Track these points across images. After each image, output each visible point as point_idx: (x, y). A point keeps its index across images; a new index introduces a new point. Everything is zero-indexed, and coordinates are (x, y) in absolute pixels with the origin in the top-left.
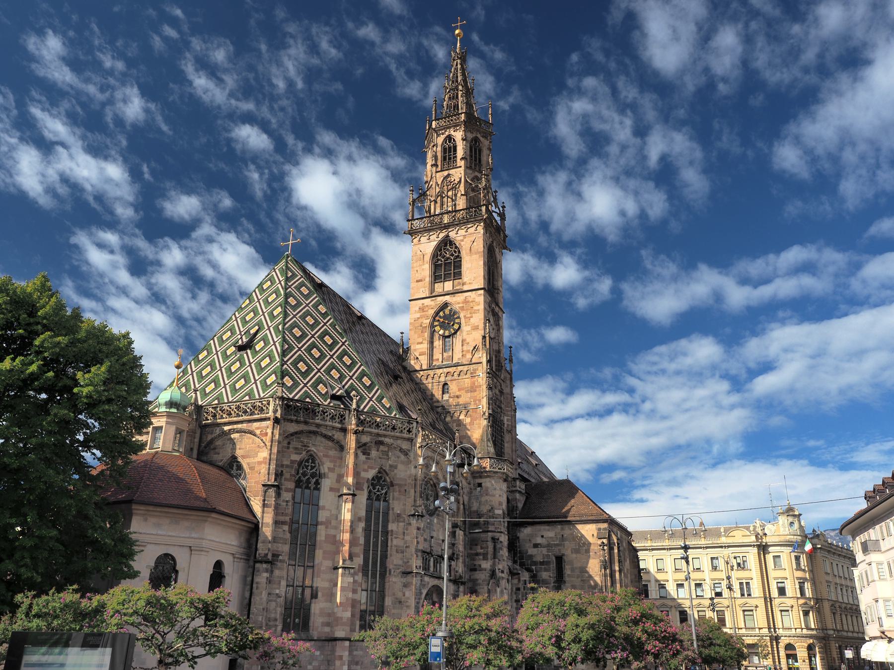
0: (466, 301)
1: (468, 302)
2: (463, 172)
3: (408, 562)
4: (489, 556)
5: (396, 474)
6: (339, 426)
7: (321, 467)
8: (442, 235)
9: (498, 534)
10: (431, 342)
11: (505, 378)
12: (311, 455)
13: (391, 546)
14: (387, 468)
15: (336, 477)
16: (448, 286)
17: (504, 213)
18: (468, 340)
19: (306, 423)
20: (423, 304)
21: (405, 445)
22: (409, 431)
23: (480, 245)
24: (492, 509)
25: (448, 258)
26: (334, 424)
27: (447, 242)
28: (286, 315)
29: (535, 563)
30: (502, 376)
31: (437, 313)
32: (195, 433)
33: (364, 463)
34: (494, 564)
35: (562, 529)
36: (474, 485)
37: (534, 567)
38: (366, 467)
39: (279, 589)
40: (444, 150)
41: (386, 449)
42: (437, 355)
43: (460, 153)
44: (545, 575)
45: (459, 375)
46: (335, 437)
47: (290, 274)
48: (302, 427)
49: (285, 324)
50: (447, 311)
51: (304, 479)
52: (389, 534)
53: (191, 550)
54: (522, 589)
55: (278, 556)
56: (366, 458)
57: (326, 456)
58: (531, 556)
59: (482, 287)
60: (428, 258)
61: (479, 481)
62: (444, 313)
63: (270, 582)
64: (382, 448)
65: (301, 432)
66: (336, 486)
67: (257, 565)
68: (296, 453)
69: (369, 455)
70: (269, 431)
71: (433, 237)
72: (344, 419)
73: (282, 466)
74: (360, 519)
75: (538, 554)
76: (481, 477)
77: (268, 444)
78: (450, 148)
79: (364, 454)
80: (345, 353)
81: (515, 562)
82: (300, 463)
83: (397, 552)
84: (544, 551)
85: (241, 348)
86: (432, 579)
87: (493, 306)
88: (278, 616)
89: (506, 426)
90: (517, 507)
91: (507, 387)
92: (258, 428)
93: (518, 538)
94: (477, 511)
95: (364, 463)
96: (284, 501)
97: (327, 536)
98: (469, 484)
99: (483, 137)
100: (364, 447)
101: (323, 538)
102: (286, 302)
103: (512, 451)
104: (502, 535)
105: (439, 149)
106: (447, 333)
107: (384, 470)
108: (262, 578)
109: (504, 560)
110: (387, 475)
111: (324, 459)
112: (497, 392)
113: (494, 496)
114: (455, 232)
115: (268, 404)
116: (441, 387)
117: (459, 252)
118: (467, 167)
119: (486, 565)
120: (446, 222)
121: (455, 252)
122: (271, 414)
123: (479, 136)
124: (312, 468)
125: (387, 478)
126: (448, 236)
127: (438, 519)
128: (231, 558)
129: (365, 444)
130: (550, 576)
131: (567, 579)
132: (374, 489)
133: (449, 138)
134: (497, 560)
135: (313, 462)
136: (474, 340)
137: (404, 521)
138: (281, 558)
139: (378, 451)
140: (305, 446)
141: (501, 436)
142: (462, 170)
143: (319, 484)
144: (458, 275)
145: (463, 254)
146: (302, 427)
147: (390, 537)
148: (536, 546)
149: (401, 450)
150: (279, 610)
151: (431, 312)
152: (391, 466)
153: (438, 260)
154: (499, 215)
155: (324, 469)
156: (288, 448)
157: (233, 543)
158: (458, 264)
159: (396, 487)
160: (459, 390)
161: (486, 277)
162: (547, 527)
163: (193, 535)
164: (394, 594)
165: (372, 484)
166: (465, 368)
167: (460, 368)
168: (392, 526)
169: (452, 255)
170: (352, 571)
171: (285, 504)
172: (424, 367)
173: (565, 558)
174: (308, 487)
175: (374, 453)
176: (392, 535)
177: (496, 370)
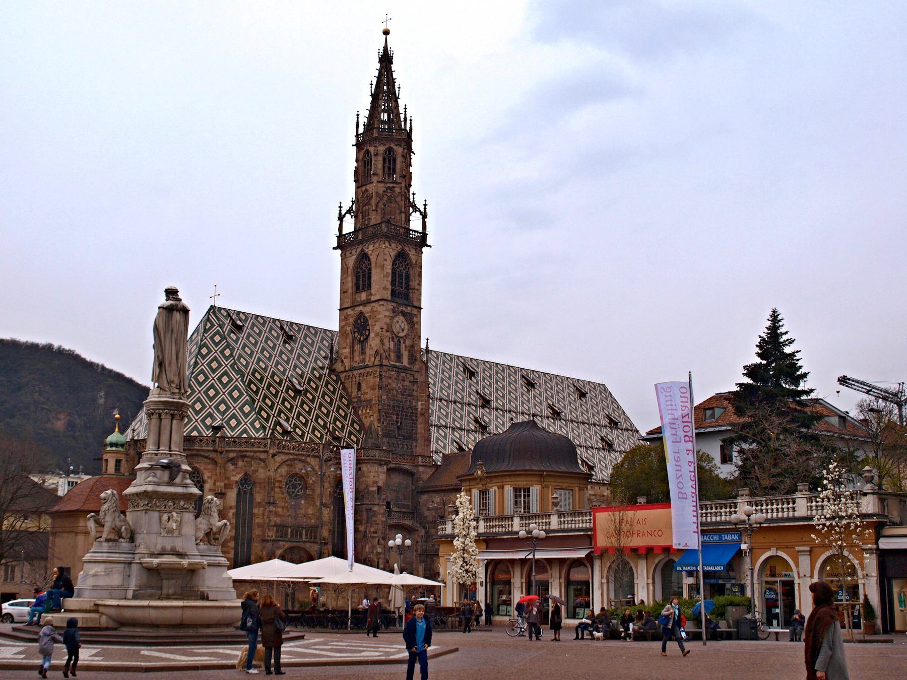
0: (372, 311)
4: (364, 522)
5: (257, 476)
9: (371, 506)
10: (353, 347)
11: (421, 368)
12: (196, 469)
15: (213, 482)
16: (363, 296)
18: (373, 345)
21: (263, 456)
22: (265, 445)
24: (367, 486)
26: (208, 448)
28: (196, 364)
29: (428, 522)
31: (356, 321)
33: (233, 470)
42: (357, 358)
45: (367, 376)
46: (211, 456)
47: (209, 325)
49: (192, 373)
64: (246, 459)
66: (213, 487)
71: (354, 252)
74: (231, 508)
80: (236, 388)
81: (417, 521)
83: (258, 527)
86: (289, 543)
89: (419, 410)
95: (233, 470)
99: (396, 145)
102: (199, 353)
106: (362, 339)
113: (368, 477)
114: (366, 247)
120: (360, 238)
123: (392, 145)
124: (198, 477)
126: (362, 250)
129: (232, 459)
132: (242, 487)
133: (368, 152)
134: (369, 525)
135: (198, 473)
136: (376, 345)
141: (413, 420)
145: (373, 265)
149: (260, 459)
151: (351, 320)
152: (253, 471)
153: (358, 272)
154: (421, 213)
155: (205, 477)
158: (370, 278)
160: (367, 388)
164: (256, 553)
165: (241, 484)
167: (367, 370)
168: (255, 511)
172: (347, 369)
175: (240, 463)
177: (409, 363)
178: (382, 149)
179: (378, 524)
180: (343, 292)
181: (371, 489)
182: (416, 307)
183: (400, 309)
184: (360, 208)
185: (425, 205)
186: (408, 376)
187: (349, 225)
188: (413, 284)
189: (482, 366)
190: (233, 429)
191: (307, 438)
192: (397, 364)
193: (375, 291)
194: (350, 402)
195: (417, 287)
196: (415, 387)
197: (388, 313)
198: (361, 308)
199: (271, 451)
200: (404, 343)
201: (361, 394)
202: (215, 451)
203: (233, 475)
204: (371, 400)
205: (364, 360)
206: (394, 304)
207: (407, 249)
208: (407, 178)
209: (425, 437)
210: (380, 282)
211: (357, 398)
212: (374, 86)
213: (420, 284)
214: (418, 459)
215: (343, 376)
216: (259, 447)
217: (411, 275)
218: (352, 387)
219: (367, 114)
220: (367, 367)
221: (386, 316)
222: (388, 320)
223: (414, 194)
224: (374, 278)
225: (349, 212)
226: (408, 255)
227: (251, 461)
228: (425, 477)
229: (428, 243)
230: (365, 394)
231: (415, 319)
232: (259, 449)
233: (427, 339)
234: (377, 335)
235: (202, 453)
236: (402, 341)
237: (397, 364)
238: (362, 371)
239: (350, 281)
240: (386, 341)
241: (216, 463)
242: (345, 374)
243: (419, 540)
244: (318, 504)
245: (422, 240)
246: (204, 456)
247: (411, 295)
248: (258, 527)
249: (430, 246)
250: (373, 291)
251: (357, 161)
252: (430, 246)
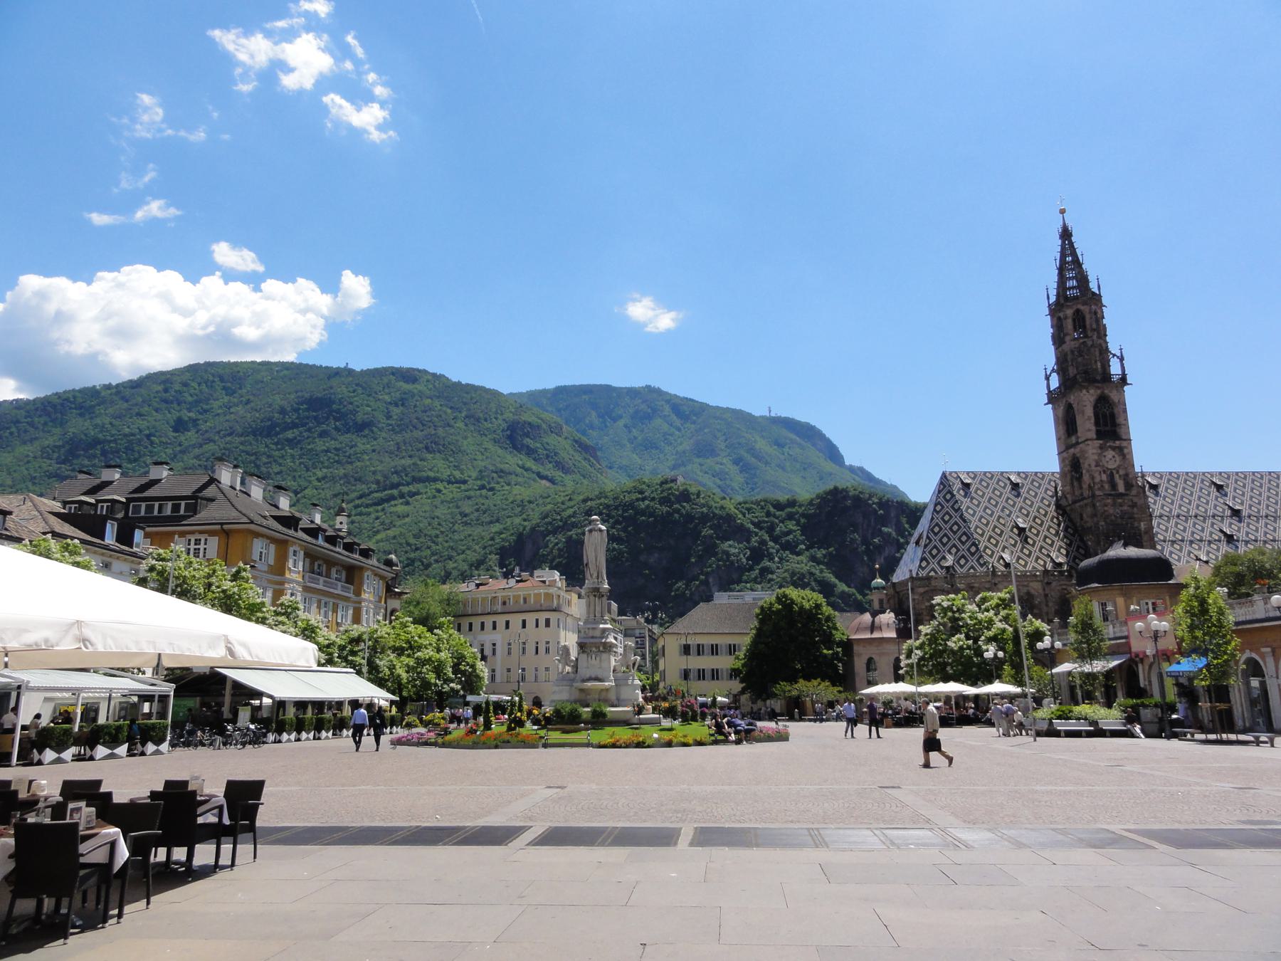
8: (1064, 402)
11: (1138, 493)
16: (1073, 439)
28: (932, 519)
42: (1077, 493)
48: (927, 588)
60: (1060, 421)
102: (935, 510)
144: (1076, 431)
145: (1076, 412)
151: (1067, 462)
154: (1118, 357)
167: (1085, 501)
177: (1126, 490)
178: (1069, 312)
180: (1058, 439)
182: (1125, 440)
184: (1062, 365)
185: (1121, 349)
187: (1055, 382)
188: (1120, 420)
189: (1233, 478)
190: (962, 567)
191: (1029, 567)
192: (1113, 492)
194: (1076, 530)
195: (1124, 422)
196: (1135, 509)
197: (1095, 451)
198: (1072, 451)
200: (1118, 472)
204: (1091, 527)
205: (1082, 494)
206: (1101, 442)
207: (1106, 391)
208: (1101, 332)
210: (1087, 425)
212: (1058, 261)
213: (1126, 419)
215: (1068, 508)
219: (1055, 285)
220: (1085, 498)
221: (1093, 454)
222: (1096, 457)
224: (1079, 422)
225: (1053, 371)
226: (1109, 397)
229: (1128, 382)
231: (1126, 451)
234: (1088, 471)
236: (1114, 472)
237: (1113, 492)
238: (1081, 503)
239: (1062, 429)
240: (1097, 475)
245: (1123, 380)
247: (1118, 430)
250: (1079, 434)
251: (1052, 327)
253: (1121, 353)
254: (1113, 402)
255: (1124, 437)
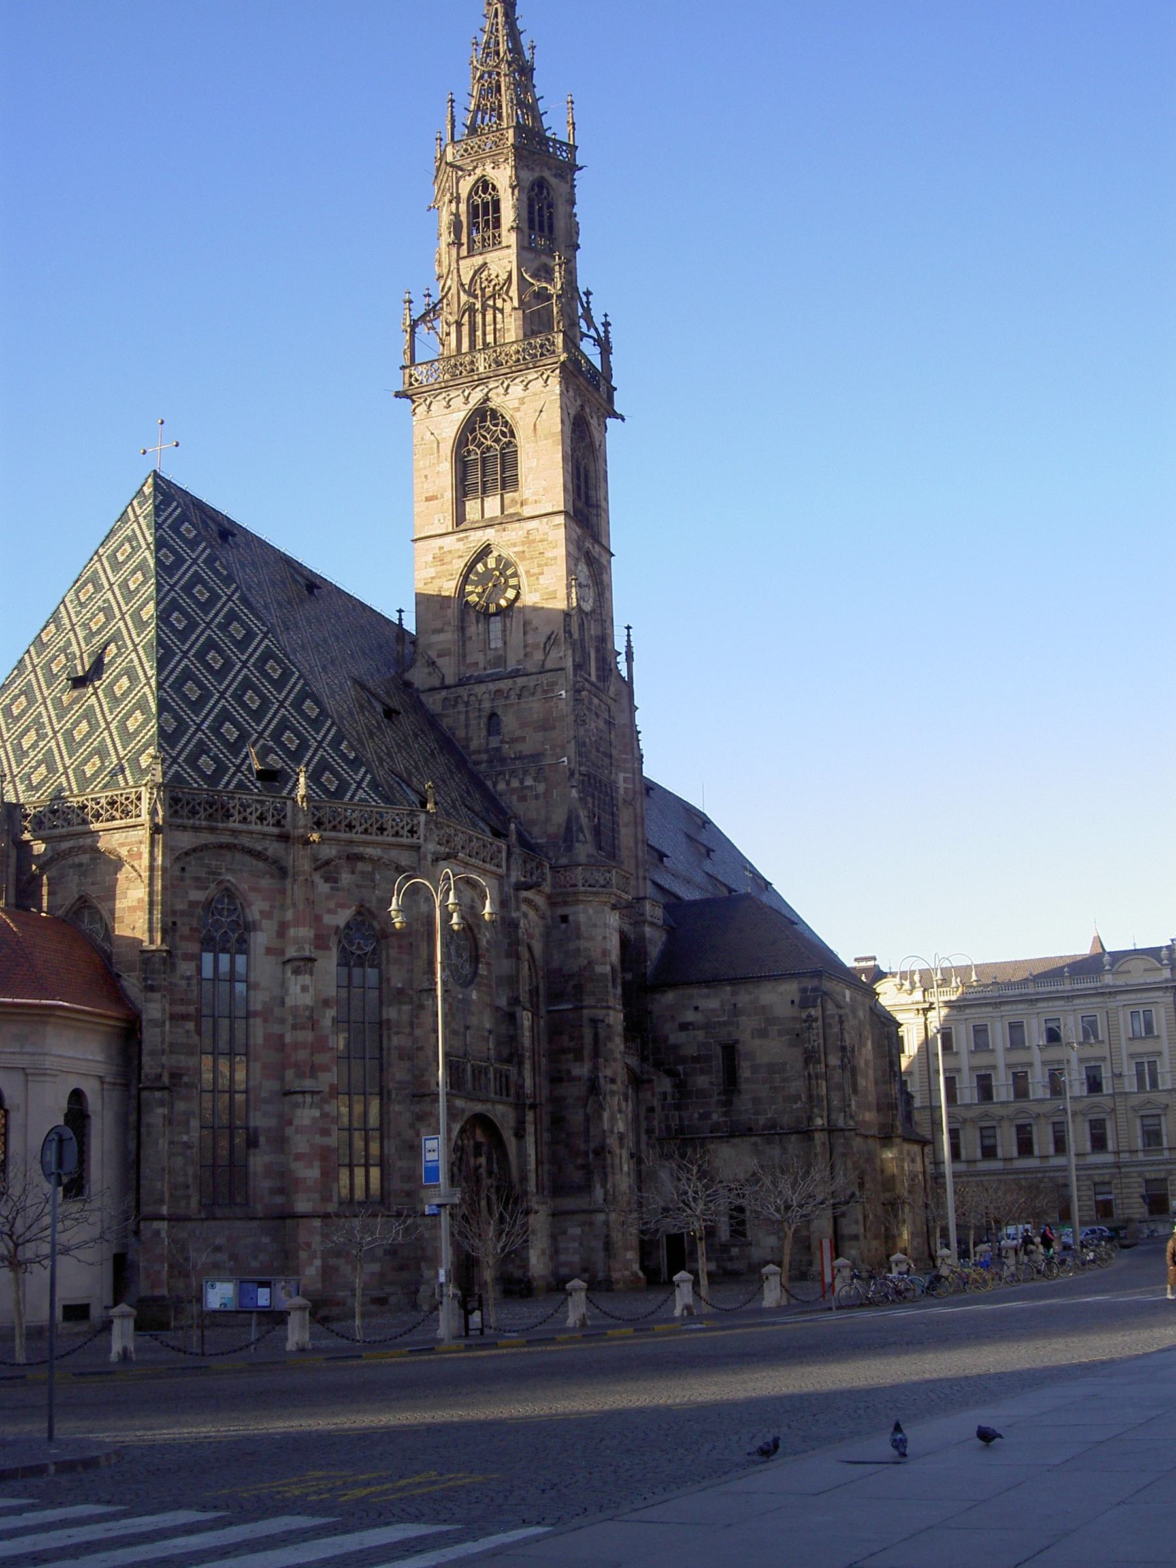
0: (528, 540)
1: (534, 541)
2: (514, 258)
3: (422, 1075)
6: (276, 830)
7: (247, 910)
9: (604, 1012)
10: (462, 629)
12: (227, 889)
13: (389, 1049)
14: (373, 905)
15: (275, 927)
16: (492, 505)
17: (607, 337)
19: (212, 830)
20: (441, 548)
22: (412, 832)
23: (553, 421)
25: (489, 448)
26: (266, 829)
27: (483, 415)
30: (612, 689)
31: (471, 567)
32: (8, 857)
33: (328, 897)
34: (596, 1068)
35: (734, 993)
36: (552, 918)
37: (680, 1068)
38: (332, 906)
39: (188, 1133)
40: (474, 211)
41: (370, 869)
43: (508, 215)
44: (702, 1081)
45: (519, 697)
46: (270, 852)
48: (206, 838)
50: (491, 563)
51: (218, 935)
52: (384, 1027)
53: (27, 1075)
54: (658, 1109)
55: (180, 1076)
56: (332, 888)
57: (253, 889)
58: (676, 1047)
59: (562, 508)
61: (561, 911)
62: (485, 565)
63: (170, 1122)
64: (360, 866)
65: (204, 848)
67: (144, 1094)
68: (197, 888)
69: (336, 881)
70: (145, 849)
72: (284, 817)
73: (174, 913)
74: (326, 1003)
75: (689, 1043)
76: (565, 903)
77: (145, 874)
78: (486, 205)
79: (327, 880)
81: (644, 1059)
82: (208, 905)
83: (401, 1058)
84: (700, 1035)
85: (79, 682)
87: (588, 544)
88: (190, 1180)
89: (622, 791)
90: (646, 953)
91: (623, 711)
92: (122, 845)
93: (650, 1012)
94: (561, 969)
95: (328, 897)
96: (182, 977)
97: (268, 1038)
98: (543, 917)
99: (555, 176)
100: (325, 868)
101: (260, 1041)
103: (636, 843)
104: (611, 1012)
105: (463, 207)
107: (369, 910)
108: (156, 1115)
109: (615, 1060)
110: (374, 917)
111: (252, 896)
112: (601, 724)
113: (591, 939)
115: (139, 799)
116: (483, 721)
117: (513, 435)
118: (522, 249)
119: (582, 1070)
121: (504, 434)
122: (145, 817)
123: (547, 174)
125: (375, 924)
127: (479, 991)
128: (95, 1084)
129: (327, 863)
130: (711, 1083)
131: (744, 1086)
133: (484, 185)
134: (601, 1060)
137: (411, 1002)
138: (185, 1079)
139: (353, 873)
140: (214, 873)
141: (613, 814)
142: (512, 254)
143: (245, 941)
144: (509, 482)
146: (206, 838)
147: (385, 1033)
148: (684, 1027)
150: (190, 1170)
151: (459, 565)
153: (469, 452)
154: (598, 342)
155: (254, 912)
156: (182, 879)
157: (98, 1058)
159: (393, 941)
160: (523, 726)
161: (570, 486)
162: (705, 991)
163: (27, 1049)
164: (399, 1134)
166: (531, 681)
167: (521, 681)
169: (497, 441)
170: (317, 1098)
171: (184, 983)
173: (740, 1046)
174: (224, 950)
175: (346, 878)
176: (388, 1029)
177: (598, 677)
179: (615, 1060)
181: (599, 969)
183: (587, 545)
186: (603, 706)
193: (534, 494)
195: (603, 503)
198: (490, 534)
199: (431, 847)
201: (502, 742)
202: (284, 838)
203: (330, 911)
204: (537, 757)
206: (578, 530)
209: (636, 857)
211: (487, 751)
214: (644, 906)
216: (397, 834)
217: (592, 474)
218: (467, 726)
223: (588, 294)
226: (588, 425)
227: (373, 873)
228: (654, 951)
229: (617, 408)
230: (514, 741)
232: (400, 839)
233: (628, 628)
235: (246, 841)
238: (504, 685)
241: (283, 872)
242: (444, 693)
243: (656, 1103)
244: (502, 1002)
246: (250, 852)
248: (401, 1058)
249: (623, 420)
252: (623, 420)
253: (606, 332)
254: (592, 444)
255: (604, 543)
